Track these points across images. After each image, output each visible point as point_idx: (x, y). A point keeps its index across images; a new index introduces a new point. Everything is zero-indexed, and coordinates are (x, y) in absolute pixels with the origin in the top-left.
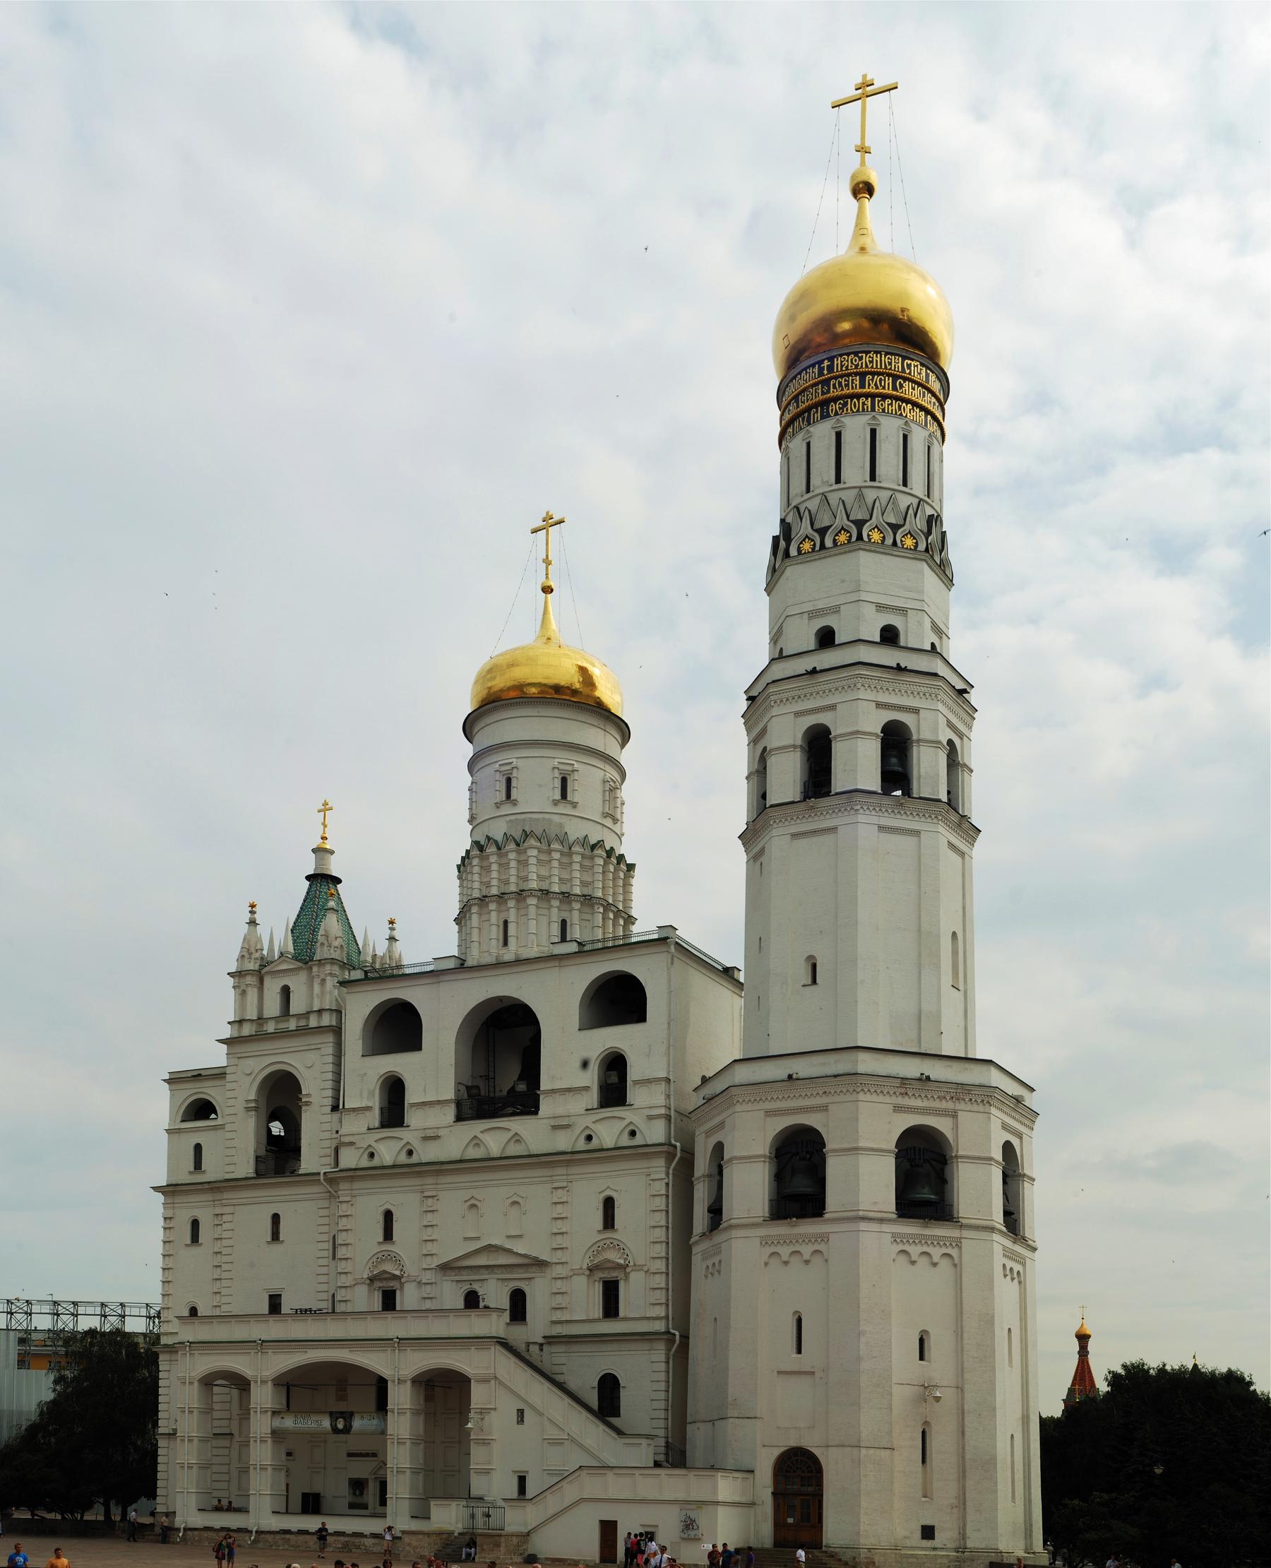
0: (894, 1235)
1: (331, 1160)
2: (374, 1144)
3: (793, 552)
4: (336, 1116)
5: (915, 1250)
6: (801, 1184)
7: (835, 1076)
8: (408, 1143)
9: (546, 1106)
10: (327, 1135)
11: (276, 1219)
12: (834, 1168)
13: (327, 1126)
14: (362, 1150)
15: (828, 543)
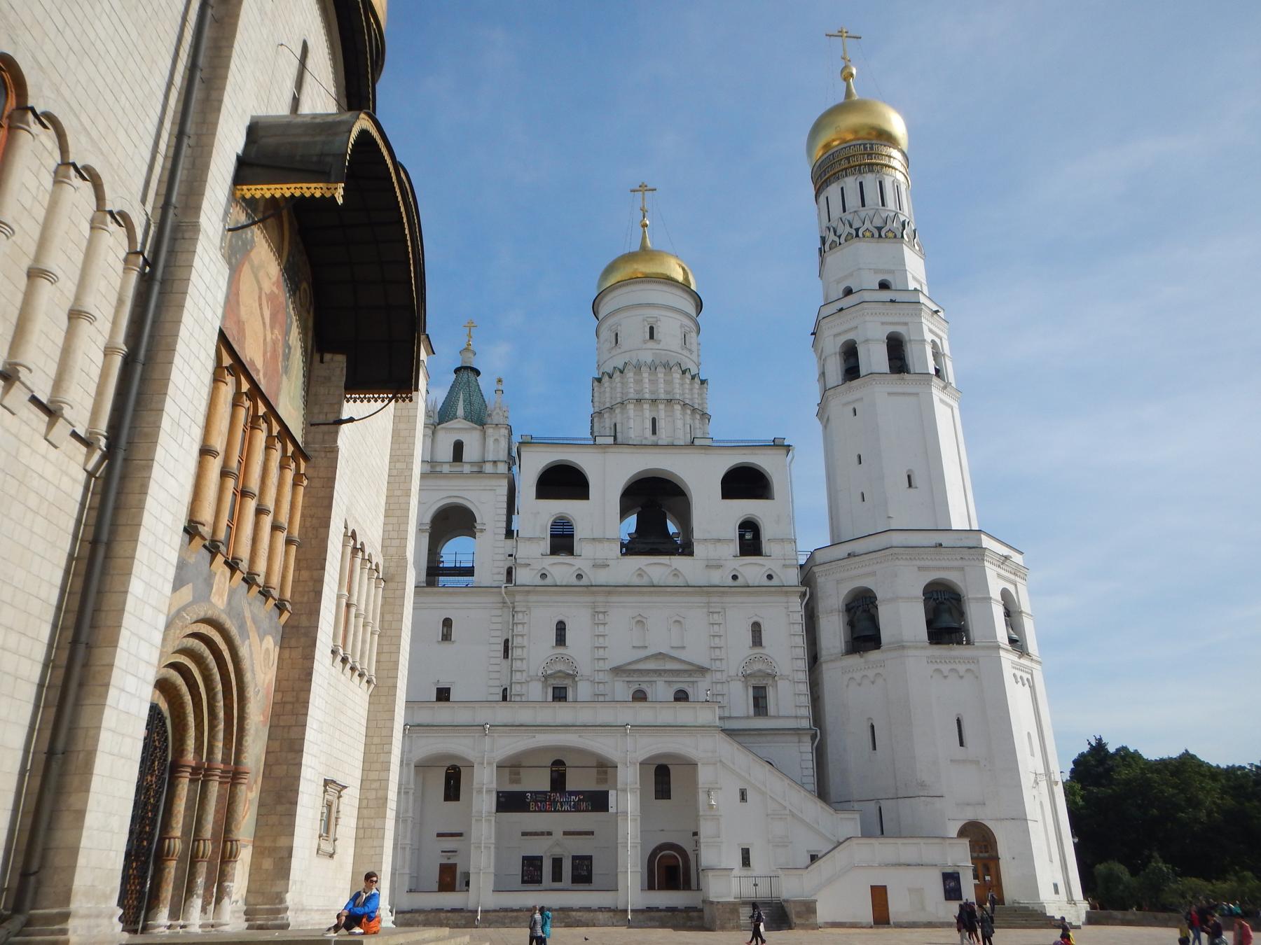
0: (1013, 662)
1: (504, 577)
2: (548, 568)
3: (860, 235)
4: (509, 542)
5: (1019, 674)
6: (946, 620)
7: (970, 548)
8: (580, 569)
9: (697, 548)
10: (502, 557)
11: (447, 623)
12: (973, 612)
13: (501, 551)
14: (536, 572)
15: (883, 234)
